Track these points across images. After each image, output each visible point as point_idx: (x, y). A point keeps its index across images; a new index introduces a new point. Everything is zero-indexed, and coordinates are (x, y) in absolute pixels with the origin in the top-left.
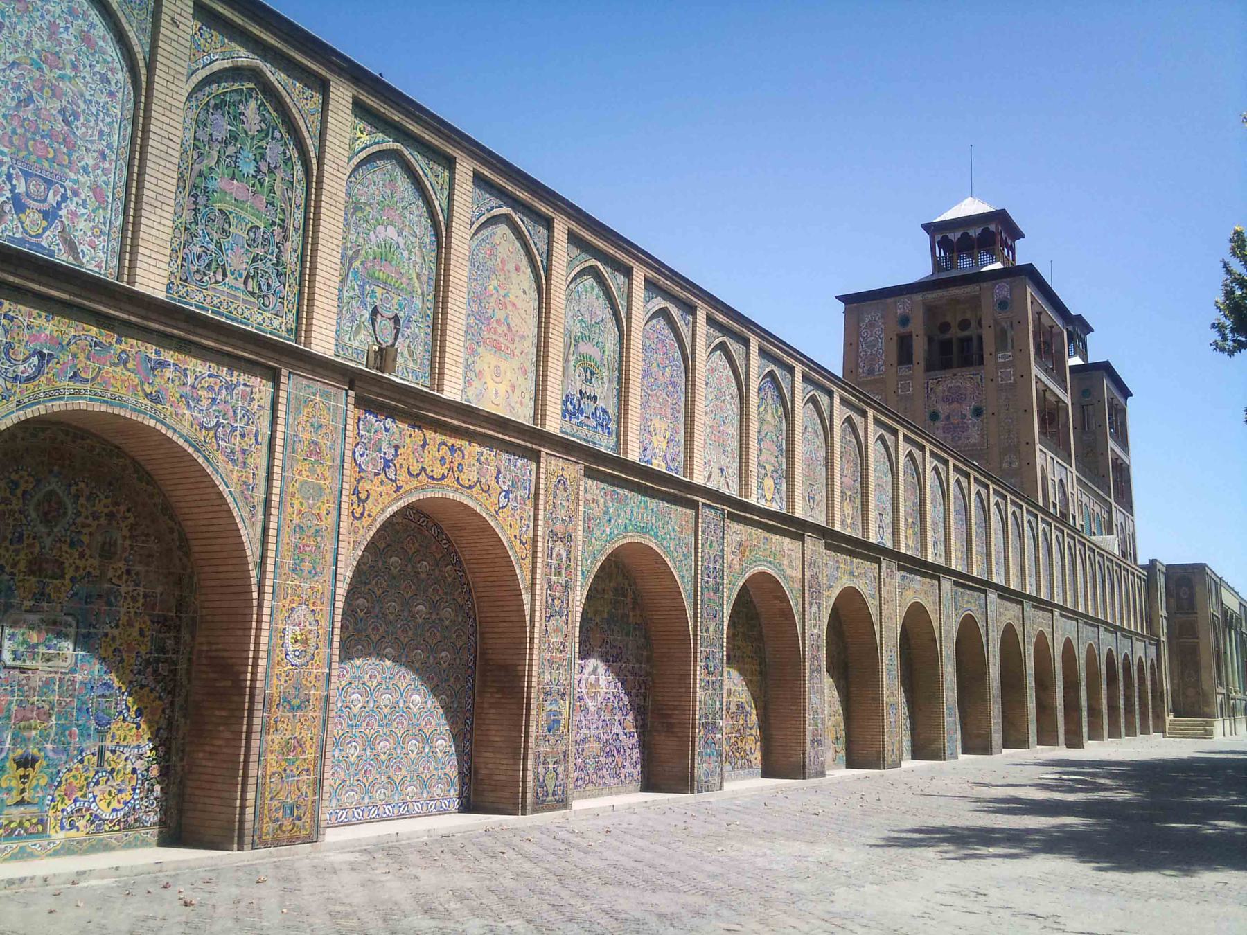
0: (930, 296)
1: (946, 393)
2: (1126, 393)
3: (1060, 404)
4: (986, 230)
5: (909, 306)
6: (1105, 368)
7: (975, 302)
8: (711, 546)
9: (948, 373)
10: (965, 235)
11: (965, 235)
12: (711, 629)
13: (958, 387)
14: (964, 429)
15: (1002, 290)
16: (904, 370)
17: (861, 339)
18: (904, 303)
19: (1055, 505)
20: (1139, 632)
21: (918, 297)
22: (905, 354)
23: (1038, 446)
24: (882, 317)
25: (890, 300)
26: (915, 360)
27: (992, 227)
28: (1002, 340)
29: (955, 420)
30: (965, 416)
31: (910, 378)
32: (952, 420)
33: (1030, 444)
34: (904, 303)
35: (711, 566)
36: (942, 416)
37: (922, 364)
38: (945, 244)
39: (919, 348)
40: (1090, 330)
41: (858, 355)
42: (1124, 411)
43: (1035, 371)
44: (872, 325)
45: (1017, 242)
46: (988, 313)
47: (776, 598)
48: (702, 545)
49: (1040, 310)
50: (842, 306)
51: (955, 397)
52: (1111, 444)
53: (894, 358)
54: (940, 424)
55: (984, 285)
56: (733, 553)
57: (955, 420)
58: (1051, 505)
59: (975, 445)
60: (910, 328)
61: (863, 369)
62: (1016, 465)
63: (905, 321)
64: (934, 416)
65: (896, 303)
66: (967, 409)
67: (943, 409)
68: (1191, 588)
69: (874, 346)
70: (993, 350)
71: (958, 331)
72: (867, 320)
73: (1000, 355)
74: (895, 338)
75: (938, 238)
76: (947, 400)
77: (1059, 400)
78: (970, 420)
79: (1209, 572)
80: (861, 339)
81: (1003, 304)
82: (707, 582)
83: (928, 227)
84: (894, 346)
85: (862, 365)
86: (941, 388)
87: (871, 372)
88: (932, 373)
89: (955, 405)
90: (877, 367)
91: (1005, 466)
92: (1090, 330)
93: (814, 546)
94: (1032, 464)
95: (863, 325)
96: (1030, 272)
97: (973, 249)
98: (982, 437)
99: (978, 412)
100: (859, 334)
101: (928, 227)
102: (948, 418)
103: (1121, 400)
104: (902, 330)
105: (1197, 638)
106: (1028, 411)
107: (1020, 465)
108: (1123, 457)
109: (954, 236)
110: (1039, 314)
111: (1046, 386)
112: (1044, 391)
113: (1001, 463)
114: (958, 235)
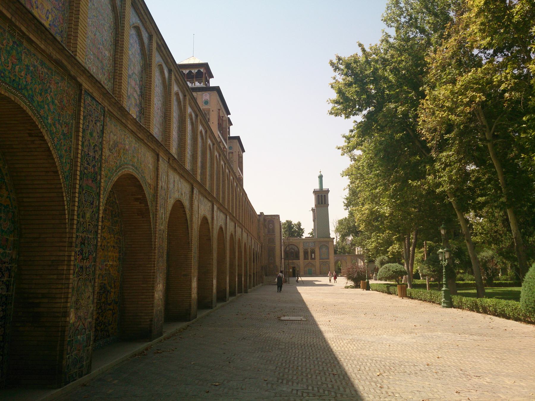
6: (238, 138)
8: (91, 134)
12: (88, 215)
35: (91, 154)
40: (232, 125)
45: (210, 79)
47: (137, 200)
48: (84, 130)
55: (199, 93)
56: (110, 150)
77: (225, 147)
82: (86, 168)
92: (232, 125)
93: (163, 166)
96: (217, 89)
97: (193, 78)
112: (220, 142)
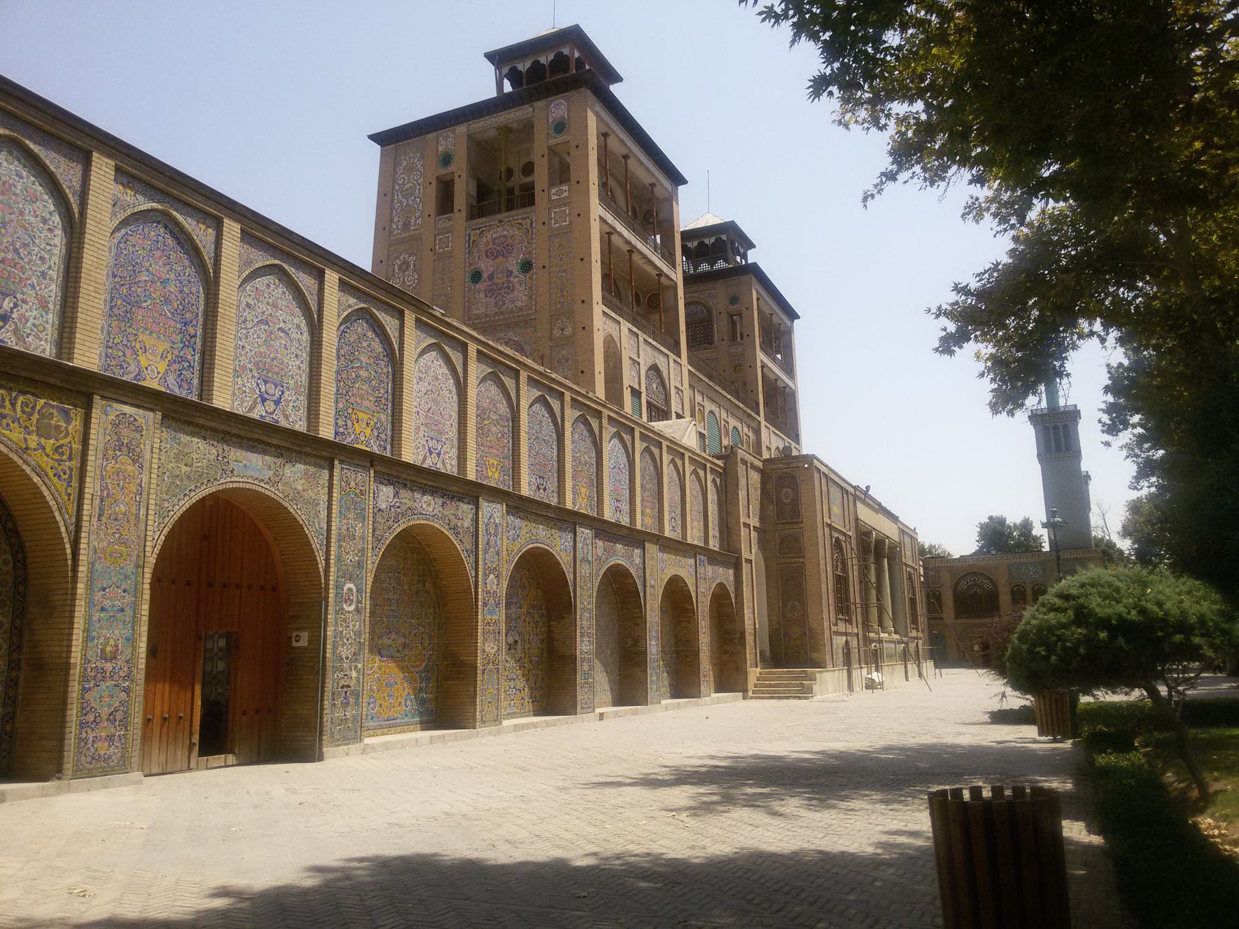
0: (476, 126)
1: (489, 247)
2: (793, 315)
3: (663, 279)
4: (559, 56)
5: (454, 141)
7: (528, 127)
9: (493, 220)
10: (536, 63)
11: (536, 63)
13: (505, 236)
14: (511, 289)
15: (558, 108)
16: (443, 222)
17: (397, 187)
18: (446, 138)
19: (636, 393)
20: (714, 544)
21: (462, 129)
22: (445, 203)
23: (598, 308)
24: (422, 157)
25: (430, 136)
26: (457, 206)
27: (566, 51)
28: (562, 173)
29: (500, 278)
30: (511, 272)
31: (448, 231)
32: (495, 281)
33: (586, 302)
34: (446, 138)
36: (485, 275)
37: (464, 214)
38: (515, 76)
39: (463, 192)
41: (392, 208)
42: (789, 332)
43: (597, 209)
44: (410, 169)
46: (542, 142)
49: (625, 152)
50: (376, 149)
51: (500, 250)
52: (761, 356)
53: (431, 207)
54: (481, 286)
55: (539, 104)
57: (500, 278)
58: (627, 394)
59: (521, 309)
60: (452, 168)
61: (397, 227)
62: (568, 332)
63: (446, 159)
64: (476, 276)
65: (437, 138)
66: (513, 264)
67: (486, 266)
68: (795, 488)
69: (411, 194)
70: (546, 187)
71: (521, 176)
72: (404, 164)
73: (553, 191)
74: (434, 184)
75: (506, 70)
76: (491, 254)
77: (661, 274)
78: (518, 277)
79: (823, 469)
80: (397, 187)
81: (560, 127)
83: (491, 56)
84: (432, 192)
85: (396, 219)
86: (484, 240)
87: (406, 226)
88: (474, 222)
89: (500, 259)
90: (413, 221)
91: (557, 333)
94: (587, 329)
95: (400, 170)
98: (530, 298)
99: (527, 266)
100: (395, 181)
101: (491, 56)
102: (491, 277)
103: (789, 323)
104: (443, 171)
105: (803, 557)
106: (585, 259)
107: (574, 329)
108: (790, 384)
109: (524, 66)
110: (605, 135)
111: (628, 242)
112: (631, 252)
113: (551, 330)
114: (528, 64)
